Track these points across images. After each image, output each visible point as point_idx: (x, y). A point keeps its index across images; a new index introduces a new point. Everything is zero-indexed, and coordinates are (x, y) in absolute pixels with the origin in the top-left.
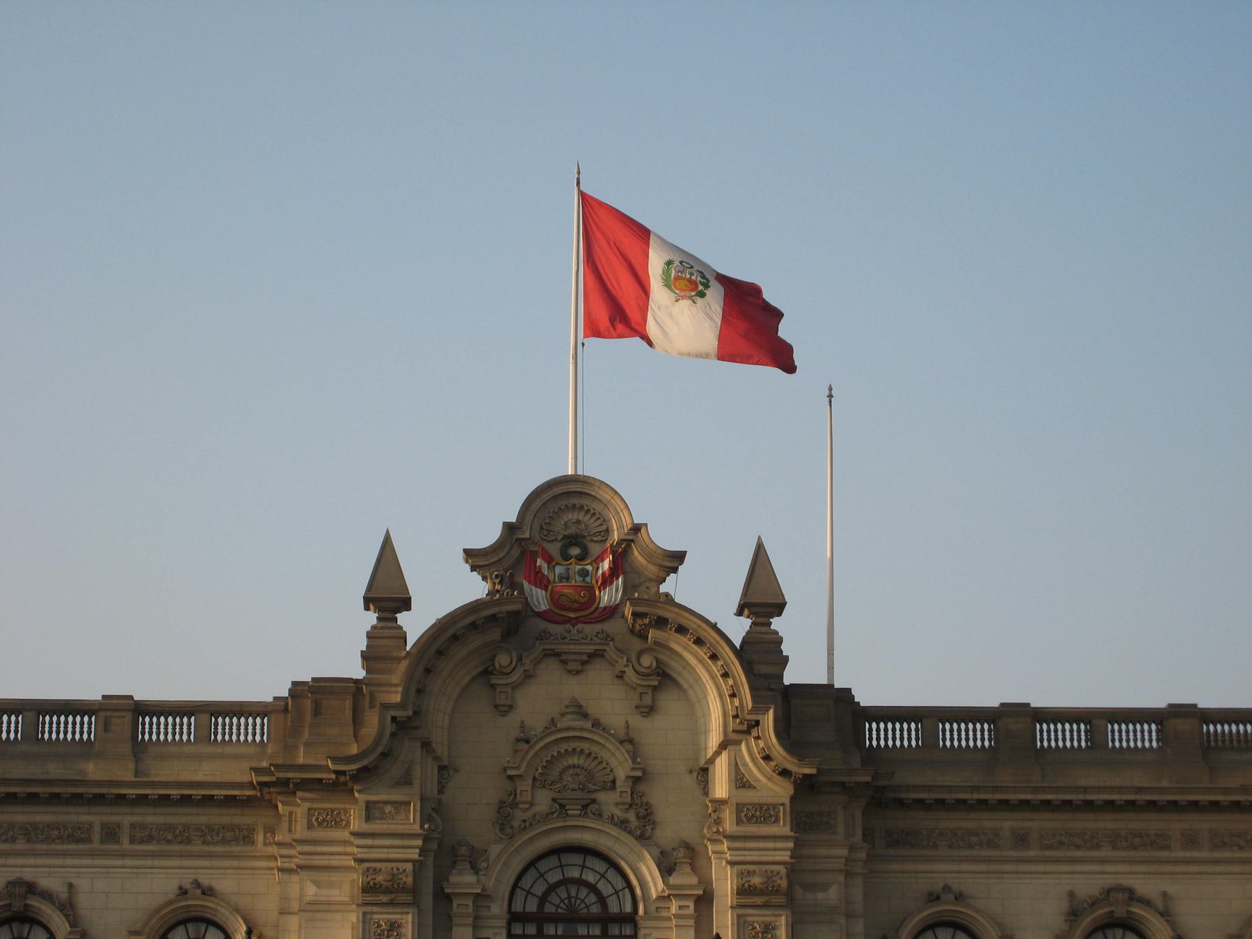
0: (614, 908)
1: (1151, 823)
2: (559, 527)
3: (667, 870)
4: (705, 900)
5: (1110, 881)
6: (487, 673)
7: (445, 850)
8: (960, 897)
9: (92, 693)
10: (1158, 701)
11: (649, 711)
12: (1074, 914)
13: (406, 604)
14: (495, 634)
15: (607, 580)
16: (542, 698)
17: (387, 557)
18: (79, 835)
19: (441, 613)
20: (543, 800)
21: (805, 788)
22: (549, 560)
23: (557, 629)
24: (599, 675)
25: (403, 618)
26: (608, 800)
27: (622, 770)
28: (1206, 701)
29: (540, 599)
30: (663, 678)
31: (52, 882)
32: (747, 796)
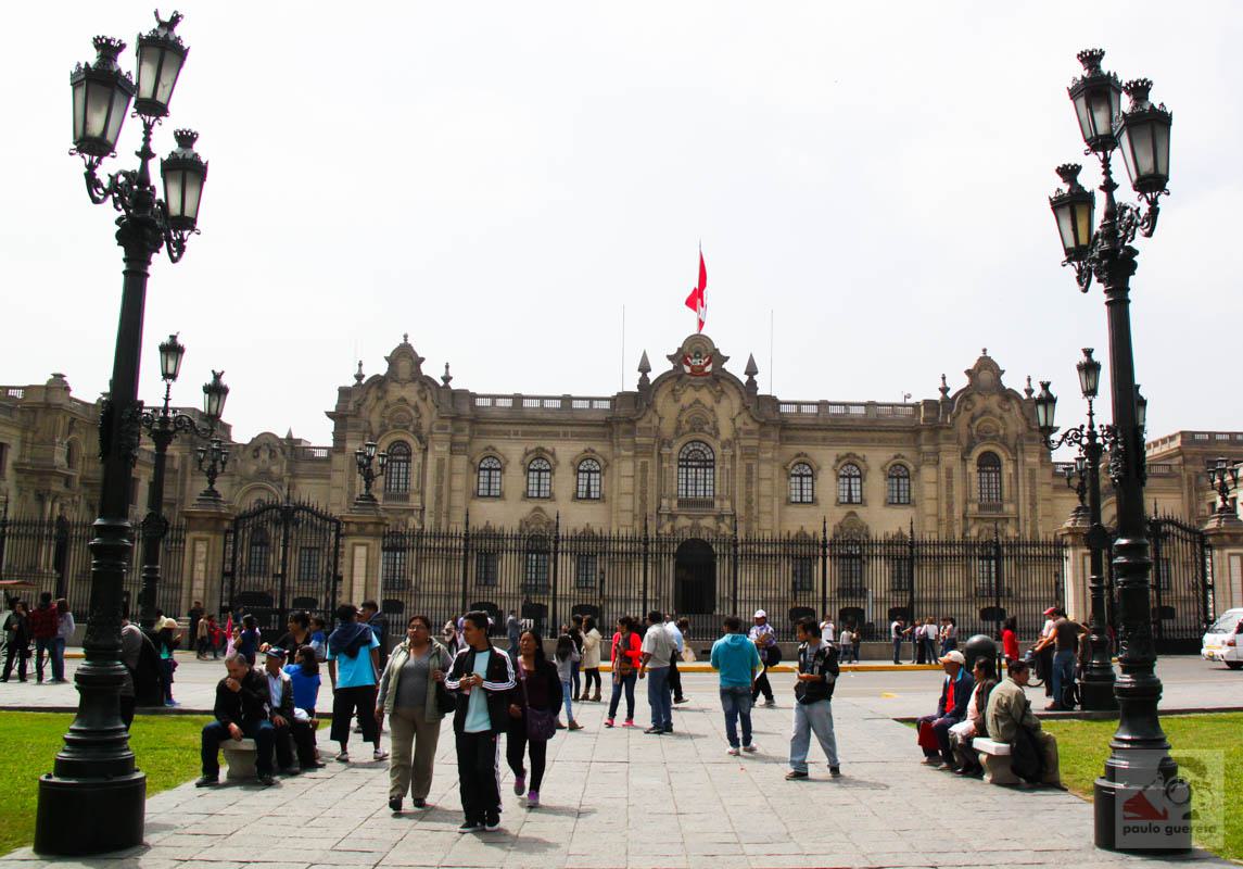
0: (708, 457)
3: (723, 447)
4: (734, 456)
5: (848, 451)
6: (673, 390)
8: (806, 456)
9: (560, 394)
10: (865, 400)
11: (718, 402)
12: (838, 461)
14: (675, 380)
15: (707, 364)
16: (688, 397)
17: (645, 358)
18: (556, 435)
19: (662, 372)
20: (687, 427)
22: (691, 359)
23: (693, 378)
24: (705, 391)
25: (649, 374)
26: (706, 428)
27: (711, 418)
28: (878, 401)
29: (687, 369)
31: (549, 448)
32: (748, 428)
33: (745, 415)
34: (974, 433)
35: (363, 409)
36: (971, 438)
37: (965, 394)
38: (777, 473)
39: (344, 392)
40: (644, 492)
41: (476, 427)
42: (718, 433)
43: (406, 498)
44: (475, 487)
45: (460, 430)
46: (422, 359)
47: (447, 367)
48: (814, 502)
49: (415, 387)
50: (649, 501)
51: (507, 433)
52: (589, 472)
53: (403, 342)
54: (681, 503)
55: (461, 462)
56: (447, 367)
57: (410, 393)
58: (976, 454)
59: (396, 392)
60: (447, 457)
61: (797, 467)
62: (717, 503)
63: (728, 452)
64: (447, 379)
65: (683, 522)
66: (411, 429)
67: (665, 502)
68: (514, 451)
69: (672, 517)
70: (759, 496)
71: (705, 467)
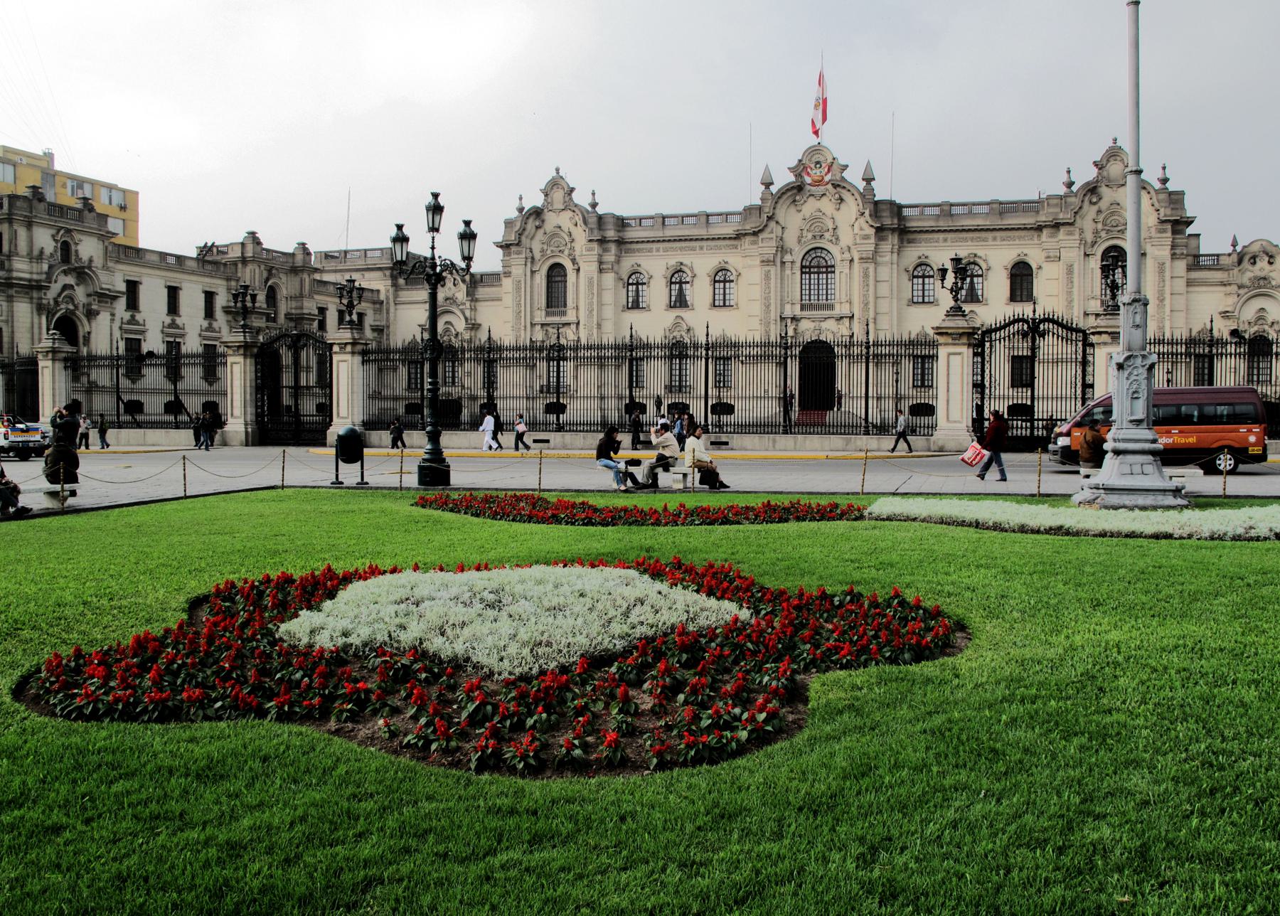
1: (983, 235)
4: (852, 261)
7: (782, 249)
10: (988, 200)
13: (772, 184)
16: (810, 207)
18: (693, 249)
20: (810, 236)
21: (879, 230)
29: (808, 180)
30: (841, 200)
33: (862, 220)
34: (1100, 226)
35: (523, 238)
36: (1096, 232)
37: (1092, 190)
38: (895, 275)
39: (509, 224)
40: (767, 298)
41: (623, 247)
42: (837, 239)
43: (564, 314)
45: (605, 250)
46: (572, 190)
47: (593, 194)
49: (569, 214)
50: (772, 307)
51: (650, 250)
52: (725, 281)
53: (554, 174)
54: (803, 308)
55: (609, 278)
56: (593, 194)
57: (565, 220)
58: (1099, 250)
59: (551, 220)
60: (595, 275)
62: (837, 306)
63: (847, 256)
64: (594, 205)
65: (805, 325)
66: (566, 252)
67: (788, 307)
68: (656, 265)
69: (794, 319)
70: (876, 298)
71: (827, 273)
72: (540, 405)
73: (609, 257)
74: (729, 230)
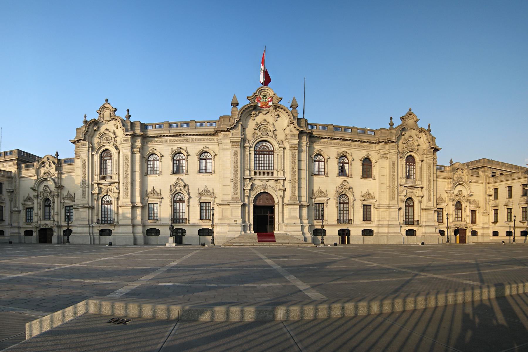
2: (262, 94)
18: (187, 141)
29: (259, 105)
43: (110, 177)
44: (146, 171)
48: (326, 175)
60: (129, 155)
61: (316, 157)
72: (97, 230)
73: (138, 144)
74: (211, 130)
